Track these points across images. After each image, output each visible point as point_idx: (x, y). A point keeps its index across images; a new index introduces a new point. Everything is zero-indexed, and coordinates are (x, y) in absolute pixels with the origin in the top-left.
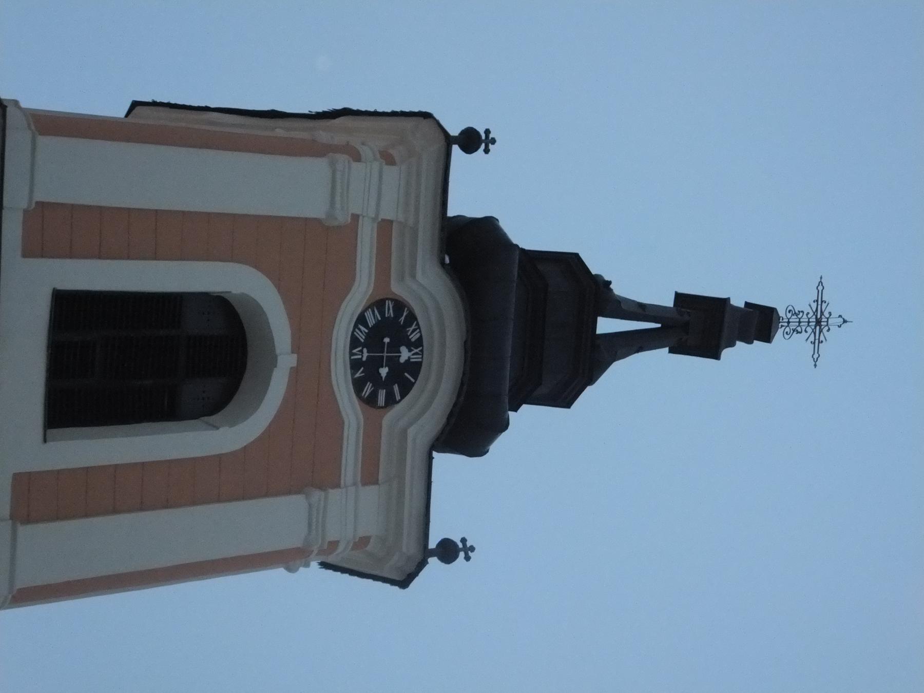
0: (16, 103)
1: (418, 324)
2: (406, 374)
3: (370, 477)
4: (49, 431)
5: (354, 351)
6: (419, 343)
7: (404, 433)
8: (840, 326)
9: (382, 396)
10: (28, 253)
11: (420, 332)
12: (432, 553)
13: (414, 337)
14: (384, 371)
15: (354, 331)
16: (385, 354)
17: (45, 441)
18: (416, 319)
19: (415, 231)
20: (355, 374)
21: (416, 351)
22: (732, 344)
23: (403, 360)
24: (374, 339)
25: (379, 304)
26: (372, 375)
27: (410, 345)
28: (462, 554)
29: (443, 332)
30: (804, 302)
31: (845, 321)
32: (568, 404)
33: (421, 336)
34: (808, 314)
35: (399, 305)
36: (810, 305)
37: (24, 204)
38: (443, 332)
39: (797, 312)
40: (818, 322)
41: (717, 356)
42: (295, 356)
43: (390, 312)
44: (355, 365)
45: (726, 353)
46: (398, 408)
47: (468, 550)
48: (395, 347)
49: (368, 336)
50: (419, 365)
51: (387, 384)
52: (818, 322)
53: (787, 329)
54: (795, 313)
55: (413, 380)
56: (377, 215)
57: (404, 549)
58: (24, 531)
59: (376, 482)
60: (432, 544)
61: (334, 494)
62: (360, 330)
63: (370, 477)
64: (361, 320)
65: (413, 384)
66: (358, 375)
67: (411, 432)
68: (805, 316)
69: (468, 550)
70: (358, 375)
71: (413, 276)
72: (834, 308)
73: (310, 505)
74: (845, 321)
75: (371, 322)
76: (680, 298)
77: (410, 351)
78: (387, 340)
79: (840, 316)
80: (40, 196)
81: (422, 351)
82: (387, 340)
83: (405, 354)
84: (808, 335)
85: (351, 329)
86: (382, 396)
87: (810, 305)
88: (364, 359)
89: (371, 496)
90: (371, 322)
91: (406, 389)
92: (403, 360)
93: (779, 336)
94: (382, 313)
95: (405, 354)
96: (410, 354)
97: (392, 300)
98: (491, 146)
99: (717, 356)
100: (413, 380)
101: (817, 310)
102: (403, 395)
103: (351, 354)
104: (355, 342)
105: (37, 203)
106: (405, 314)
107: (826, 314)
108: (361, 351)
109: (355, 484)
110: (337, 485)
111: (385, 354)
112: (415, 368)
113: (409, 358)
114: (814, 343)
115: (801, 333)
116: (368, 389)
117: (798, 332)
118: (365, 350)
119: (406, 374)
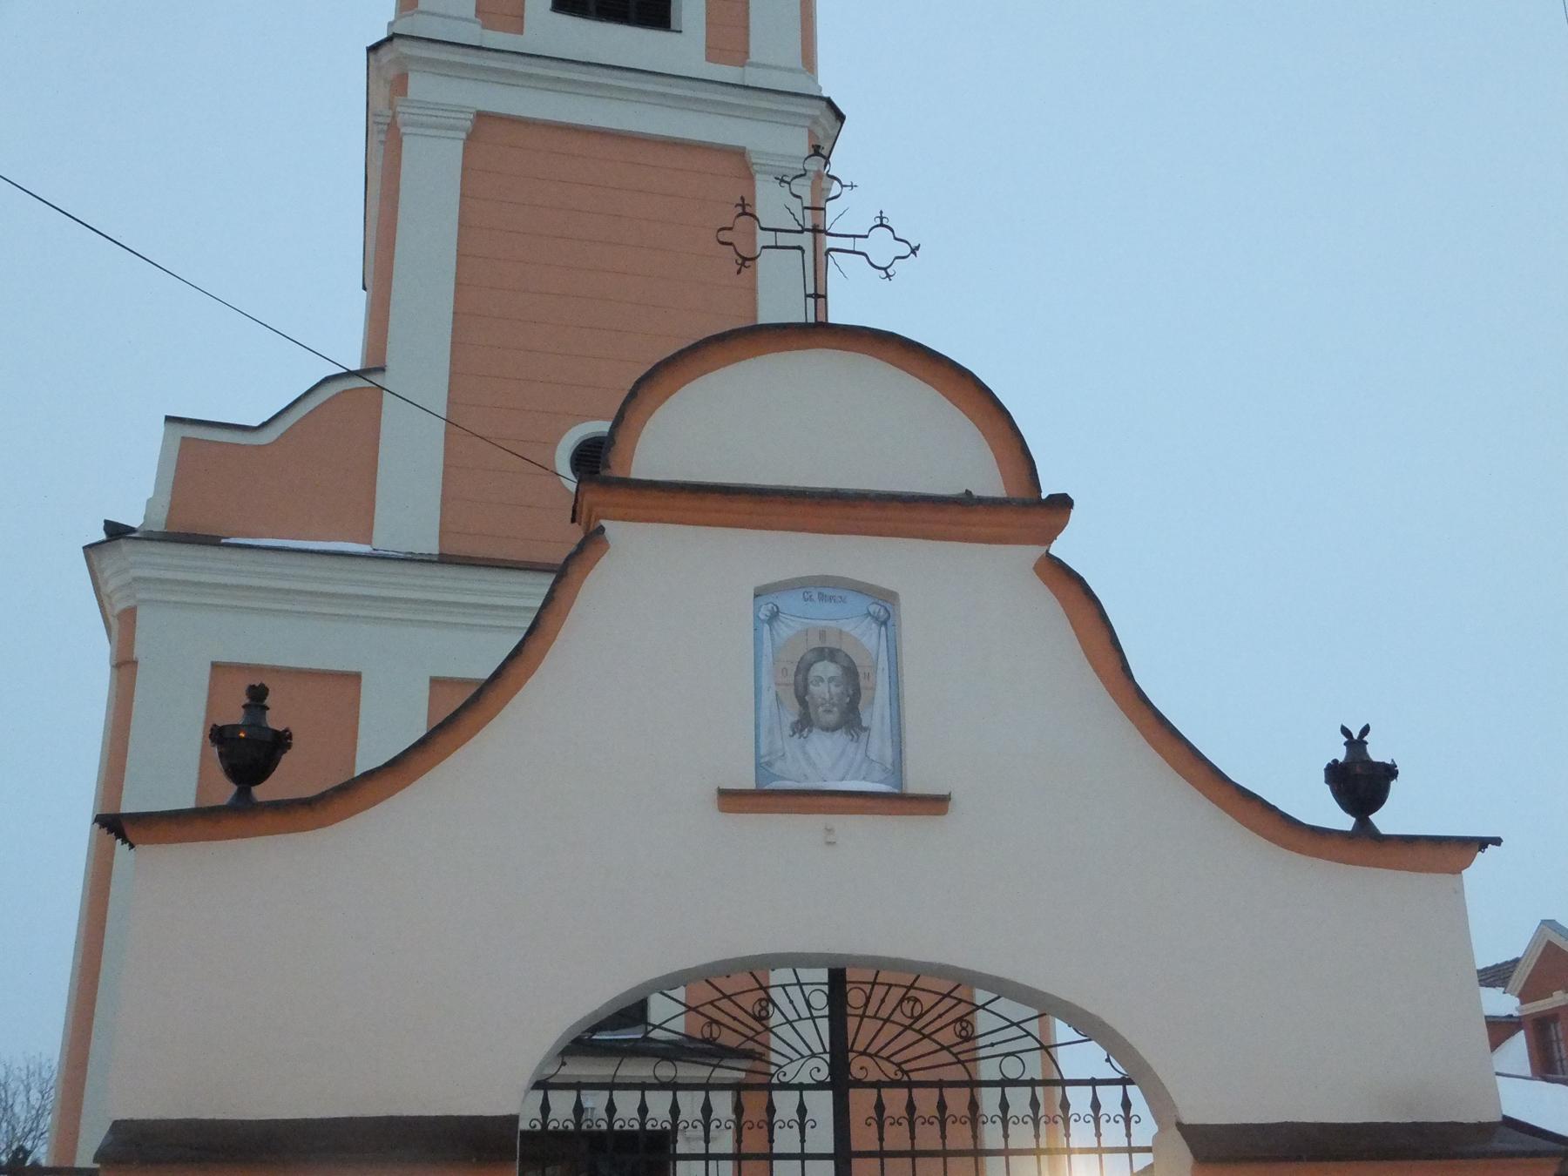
0: (390, 24)
4: (672, 28)
10: (520, 30)
17: (681, 32)
37: (477, 28)
105: (476, 16)
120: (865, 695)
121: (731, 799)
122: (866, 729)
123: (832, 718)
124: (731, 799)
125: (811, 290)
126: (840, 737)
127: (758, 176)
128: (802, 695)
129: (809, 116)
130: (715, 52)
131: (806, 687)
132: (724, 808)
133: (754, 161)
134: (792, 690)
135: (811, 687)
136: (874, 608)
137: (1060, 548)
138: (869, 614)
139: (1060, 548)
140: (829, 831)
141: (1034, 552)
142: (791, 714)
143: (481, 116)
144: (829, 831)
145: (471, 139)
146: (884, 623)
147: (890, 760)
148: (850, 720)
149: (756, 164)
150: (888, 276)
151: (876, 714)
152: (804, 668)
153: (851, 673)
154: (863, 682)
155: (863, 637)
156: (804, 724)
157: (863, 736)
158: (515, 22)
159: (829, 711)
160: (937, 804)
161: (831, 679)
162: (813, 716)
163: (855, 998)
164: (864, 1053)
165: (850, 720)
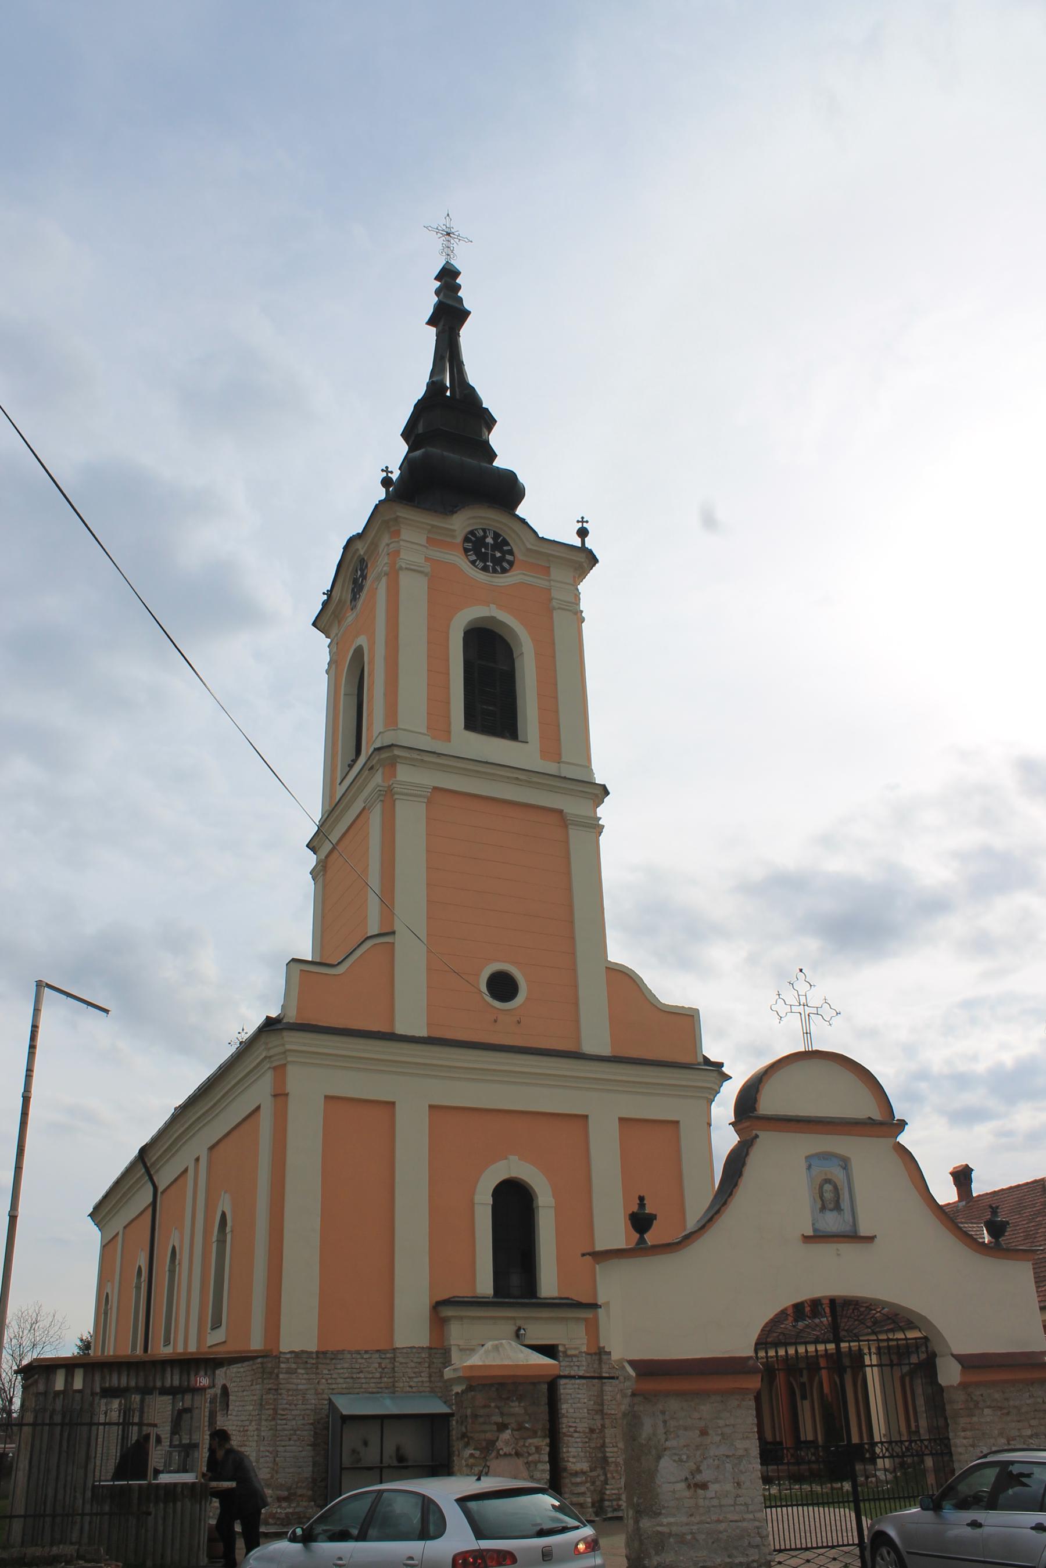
1: (476, 529)
2: (499, 541)
4: (520, 739)
6: (484, 530)
7: (529, 550)
8: (451, 220)
9: (509, 557)
11: (479, 529)
12: (583, 542)
13: (482, 533)
14: (498, 555)
15: (478, 568)
17: (527, 742)
18: (473, 530)
19: (433, 526)
20: (498, 572)
22: (460, 300)
24: (483, 557)
25: (466, 550)
26: (498, 562)
27: (485, 537)
28: (585, 525)
29: (481, 517)
30: (439, 242)
31: (448, 215)
33: (482, 529)
34: (444, 240)
36: (439, 238)
38: (481, 517)
39: (442, 248)
40: (448, 234)
41: (466, 314)
42: (491, 605)
44: (495, 571)
45: (467, 305)
46: (515, 550)
47: (582, 521)
48: (486, 545)
49: (480, 561)
51: (504, 553)
52: (448, 234)
53: (452, 256)
54: (443, 249)
56: (425, 546)
57: (583, 560)
59: (549, 567)
60: (577, 542)
61: (555, 594)
62: (478, 565)
64: (473, 563)
66: (499, 570)
67: (529, 546)
68: (445, 243)
69: (582, 521)
70: (499, 570)
71: (454, 531)
72: (441, 222)
73: (559, 608)
74: (448, 215)
75: (474, 558)
76: (431, 322)
77: (488, 537)
78: (483, 550)
79: (445, 218)
81: (489, 530)
82: (483, 550)
83: (489, 540)
84: (455, 244)
86: (509, 557)
87: (439, 238)
88: (491, 565)
91: (505, 542)
93: (457, 264)
94: (470, 550)
95: (489, 540)
96: (490, 537)
97: (464, 543)
98: (389, 470)
99: (466, 314)
101: (442, 234)
102: (508, 544)
106: (470, 536)
107: (444, 227)
109: (549, 581)
111: (490, 552)
112: (496, 536)
113: (491, 538)
114: (460, 240)
115: (453, 248)
116: (505, 565)
117: (453, 250)
118: (488, 564)
119: (499, 541)
120: (841, 1197)
121: (806, 1239)
122: (843, 1210)
123: (831, 1206)
124: (806, 1239)
125: (805, 1032)
126: (835, 1213)
127: (570, 827)
128: (821, 1197)
129: (594, 794)
130: (545, 754)
131: (822, 1194)
132: (804, 1242)
133: (568, 818)
134: (818, 1195)
135: (825, 1194)
136: (841, 1163)
137: (903, 1139)
138: (839, 1165)
139: (903, 1139)
140: (838, 1250)
141: (891, 1141)
142: (819, 1206)
144: (838, 1250)
145: (429, 802)
146: (845, 1169)
147: (851, 1224)
148: (837, 1207)
149: (570, 820)
150: (830, 1024)
151: (845, 1204)
152: (821, 1187)
153: (836, 1188)
154: (840, 1192)
155: (839, 1175)
156: (823, 1208)
157: (842, 1212)
158: (446, 734)
159: (830, 1203)
160: (871, 1239)
161: (830, 1191)
162: (826, 1205)
163: (839, 1309)
164: (843, 1330)
165: (837, 1207)
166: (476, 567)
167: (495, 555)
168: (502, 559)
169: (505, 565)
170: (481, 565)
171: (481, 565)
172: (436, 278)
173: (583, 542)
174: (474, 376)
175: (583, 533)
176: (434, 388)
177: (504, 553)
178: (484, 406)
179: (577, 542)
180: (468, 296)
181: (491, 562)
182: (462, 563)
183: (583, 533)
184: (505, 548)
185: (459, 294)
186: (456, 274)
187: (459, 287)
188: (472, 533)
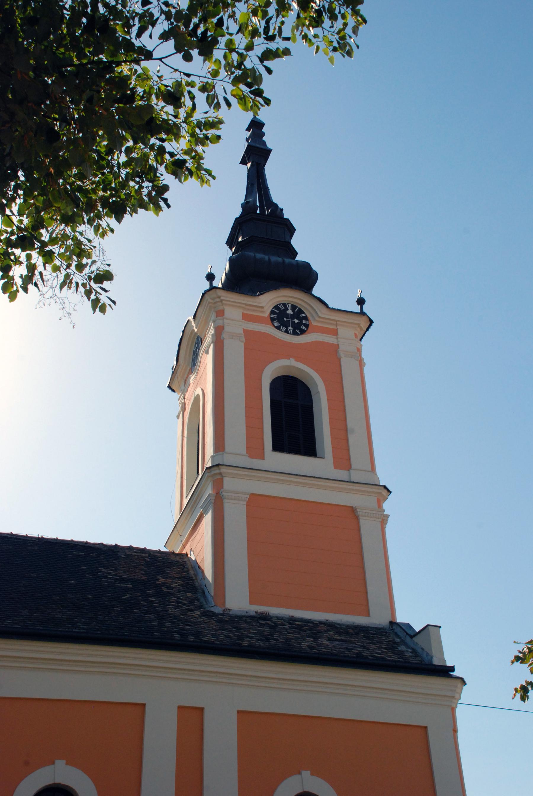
2: (296, 311)
3: (335, 333)
5: (290, 333)
6: (284, 305)
9: (304, 322)
12: (362, 309)
14: (296, 321)
15: (283, 331)
16: (290, 320)
21: (288, 307)
22: (264, 143)
23: (292, 313)
25: (272, 320)
32: (294, 230)
35: (272, 312)
41: (269, 151)
43: (275, 316)
44: (295, 333)
45: (269, 145)
48: (287, 316)
50: (293, 305)
51: (301, 319)
55: (298, 308)
58: (353, 466)
61: (342, 347)
63: (335, 333)
64: (278, 328)
65: (300, 309)
75: (278, 324)
78: (285, 319)
80: (244, 450)
81: (288, 304)
82: (285, 319)
83: (290, 312)
85: (282, 332)
86: (304, 322)
89: (342, 331)
90: (278, 324)
91: (301, 311)
92: (292, 313)
95: (290, 312)
96: (290, 309)
99: (269, 151)
100: (298, 308)
103: (291, 334)
104: (287, 332)
106: (275, 310)
108: (290, 329)
110: (338, 346)
111: (290, 320)
112: (294, 307)
116: (303, 328)
119: (296, 311)
143: (252, 494)
145: (249, 504)
166: (281, 331)
167: (294, 321)
168: (301, 323)
169: (303, 328)
170: (284, 329)
171: (284, 329)
172: (248, 129)
173: (362, 309)
174: (276, 197)
175: (361, 302)
176: (247, 207)
177: (301, 319)
178: (285, 217)
179: (357, 309)
180: (269, 140)
181: (292, 327)
182: (270, 330)
183: (361, 302)
184: (302, 315)
185: (264, 139)
186: (262, 125)
187: (263, 134)
188: (276, 307)
